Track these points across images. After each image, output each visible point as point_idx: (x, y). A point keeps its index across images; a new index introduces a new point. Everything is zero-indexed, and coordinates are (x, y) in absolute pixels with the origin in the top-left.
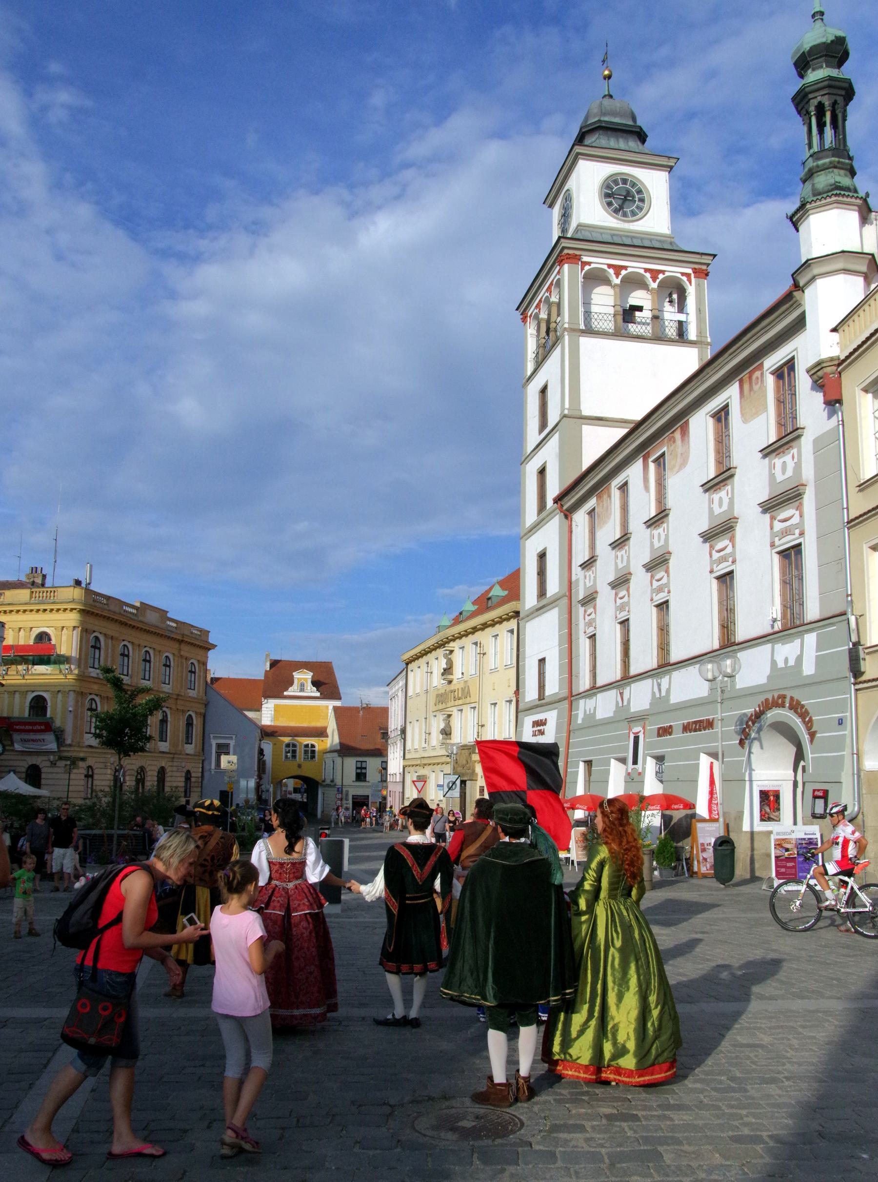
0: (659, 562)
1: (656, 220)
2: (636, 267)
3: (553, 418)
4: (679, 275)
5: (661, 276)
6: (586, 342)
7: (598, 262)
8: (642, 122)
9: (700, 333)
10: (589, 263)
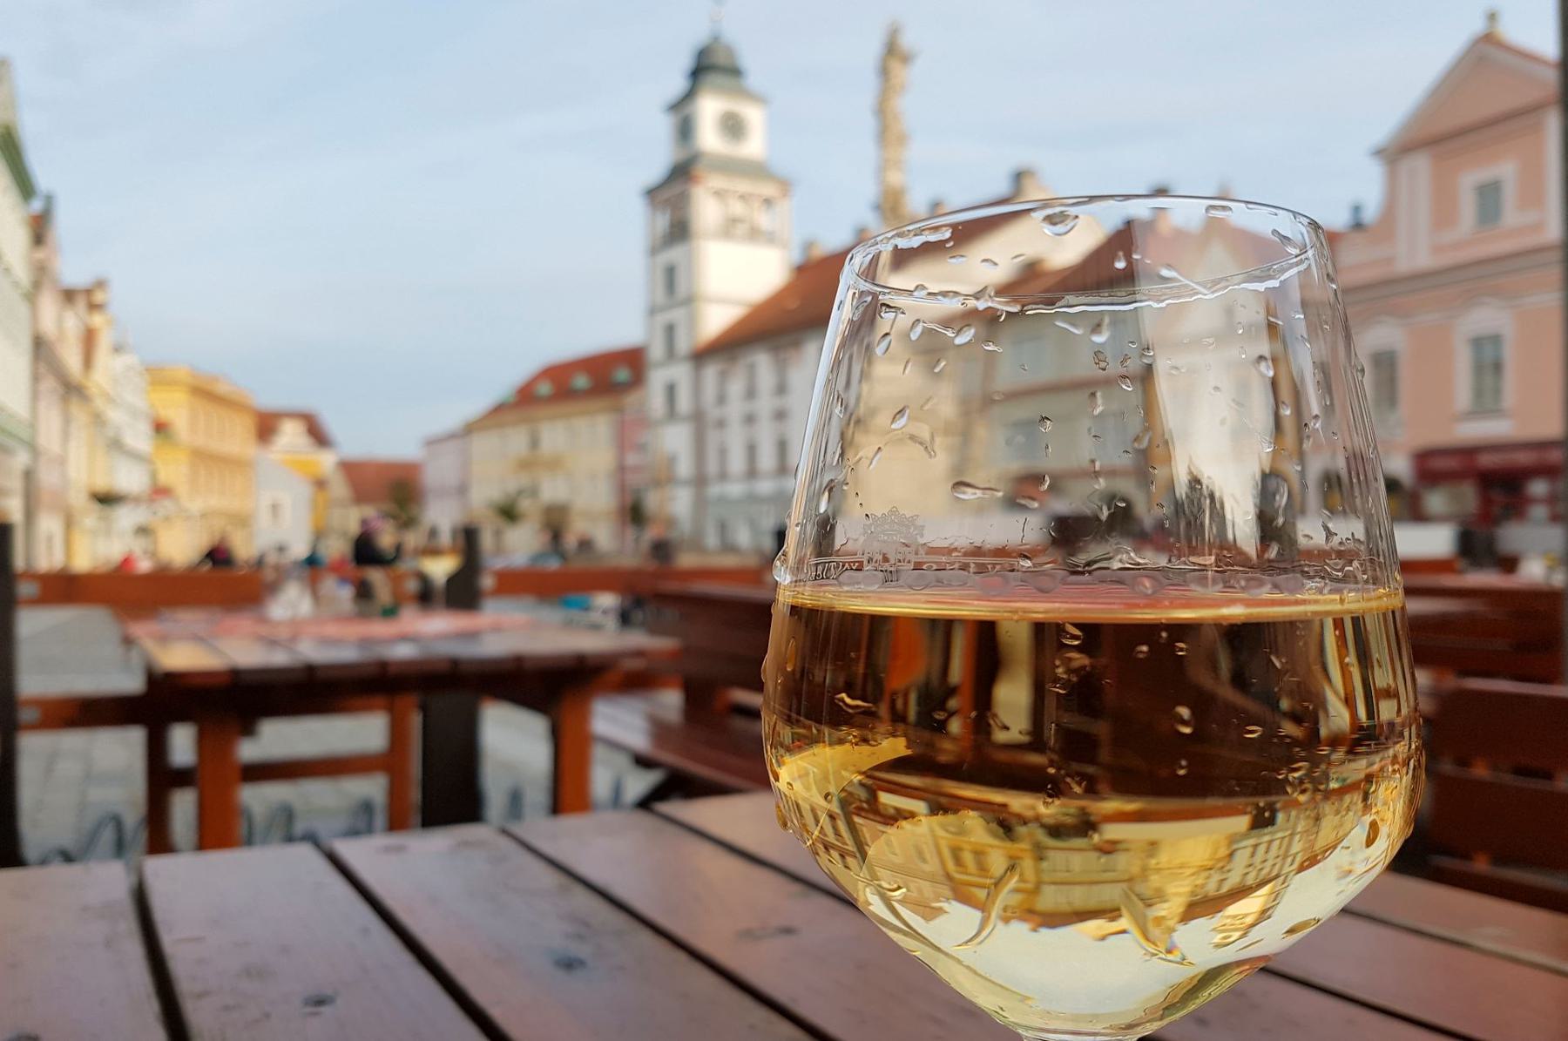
0: (780, 415)
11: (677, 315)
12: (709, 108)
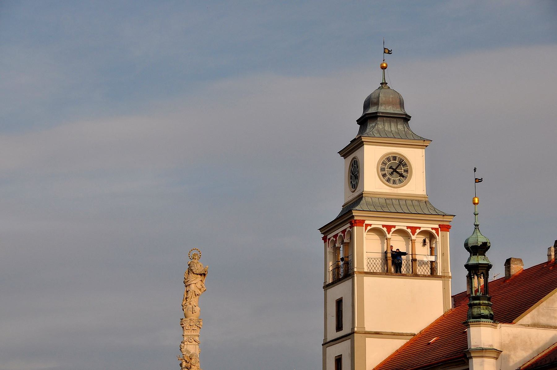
1: (416, 186)
2: (402, 225)
3: (346, 330)
4: (430, 230)
5: (418, 231)
6: (368, 280)
7: (377, 224)
8: (408, 110)
9: (443, 270)
10: (370, 225)
11: (342, 348)
12: (372, 155)
